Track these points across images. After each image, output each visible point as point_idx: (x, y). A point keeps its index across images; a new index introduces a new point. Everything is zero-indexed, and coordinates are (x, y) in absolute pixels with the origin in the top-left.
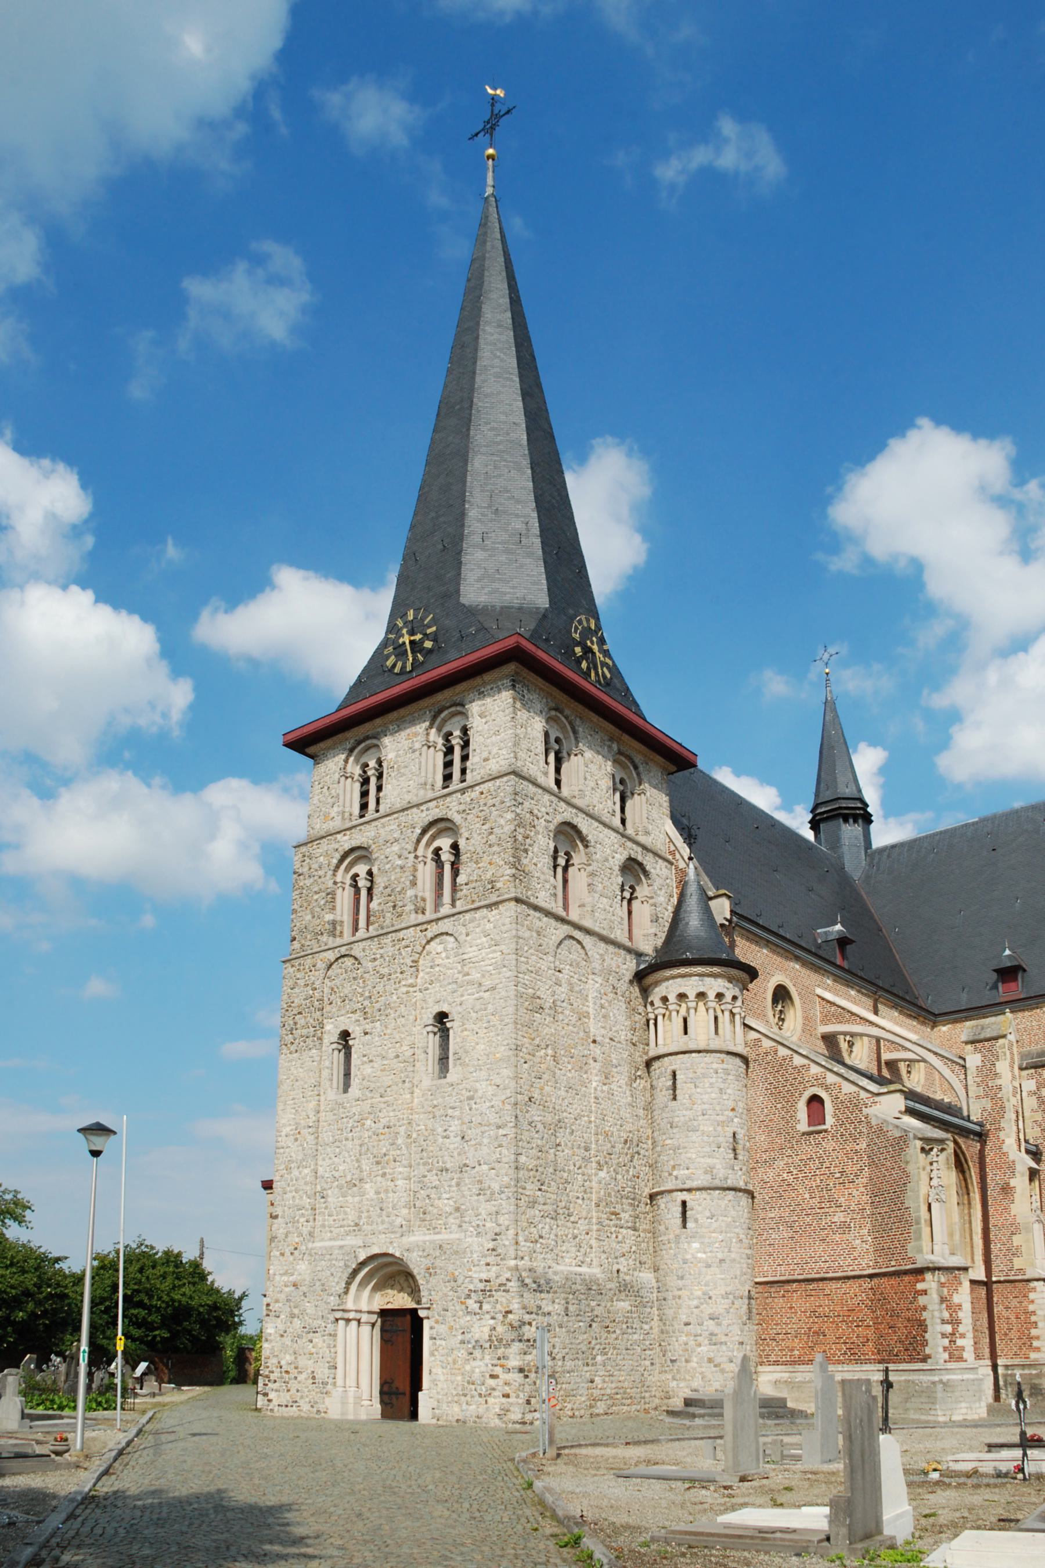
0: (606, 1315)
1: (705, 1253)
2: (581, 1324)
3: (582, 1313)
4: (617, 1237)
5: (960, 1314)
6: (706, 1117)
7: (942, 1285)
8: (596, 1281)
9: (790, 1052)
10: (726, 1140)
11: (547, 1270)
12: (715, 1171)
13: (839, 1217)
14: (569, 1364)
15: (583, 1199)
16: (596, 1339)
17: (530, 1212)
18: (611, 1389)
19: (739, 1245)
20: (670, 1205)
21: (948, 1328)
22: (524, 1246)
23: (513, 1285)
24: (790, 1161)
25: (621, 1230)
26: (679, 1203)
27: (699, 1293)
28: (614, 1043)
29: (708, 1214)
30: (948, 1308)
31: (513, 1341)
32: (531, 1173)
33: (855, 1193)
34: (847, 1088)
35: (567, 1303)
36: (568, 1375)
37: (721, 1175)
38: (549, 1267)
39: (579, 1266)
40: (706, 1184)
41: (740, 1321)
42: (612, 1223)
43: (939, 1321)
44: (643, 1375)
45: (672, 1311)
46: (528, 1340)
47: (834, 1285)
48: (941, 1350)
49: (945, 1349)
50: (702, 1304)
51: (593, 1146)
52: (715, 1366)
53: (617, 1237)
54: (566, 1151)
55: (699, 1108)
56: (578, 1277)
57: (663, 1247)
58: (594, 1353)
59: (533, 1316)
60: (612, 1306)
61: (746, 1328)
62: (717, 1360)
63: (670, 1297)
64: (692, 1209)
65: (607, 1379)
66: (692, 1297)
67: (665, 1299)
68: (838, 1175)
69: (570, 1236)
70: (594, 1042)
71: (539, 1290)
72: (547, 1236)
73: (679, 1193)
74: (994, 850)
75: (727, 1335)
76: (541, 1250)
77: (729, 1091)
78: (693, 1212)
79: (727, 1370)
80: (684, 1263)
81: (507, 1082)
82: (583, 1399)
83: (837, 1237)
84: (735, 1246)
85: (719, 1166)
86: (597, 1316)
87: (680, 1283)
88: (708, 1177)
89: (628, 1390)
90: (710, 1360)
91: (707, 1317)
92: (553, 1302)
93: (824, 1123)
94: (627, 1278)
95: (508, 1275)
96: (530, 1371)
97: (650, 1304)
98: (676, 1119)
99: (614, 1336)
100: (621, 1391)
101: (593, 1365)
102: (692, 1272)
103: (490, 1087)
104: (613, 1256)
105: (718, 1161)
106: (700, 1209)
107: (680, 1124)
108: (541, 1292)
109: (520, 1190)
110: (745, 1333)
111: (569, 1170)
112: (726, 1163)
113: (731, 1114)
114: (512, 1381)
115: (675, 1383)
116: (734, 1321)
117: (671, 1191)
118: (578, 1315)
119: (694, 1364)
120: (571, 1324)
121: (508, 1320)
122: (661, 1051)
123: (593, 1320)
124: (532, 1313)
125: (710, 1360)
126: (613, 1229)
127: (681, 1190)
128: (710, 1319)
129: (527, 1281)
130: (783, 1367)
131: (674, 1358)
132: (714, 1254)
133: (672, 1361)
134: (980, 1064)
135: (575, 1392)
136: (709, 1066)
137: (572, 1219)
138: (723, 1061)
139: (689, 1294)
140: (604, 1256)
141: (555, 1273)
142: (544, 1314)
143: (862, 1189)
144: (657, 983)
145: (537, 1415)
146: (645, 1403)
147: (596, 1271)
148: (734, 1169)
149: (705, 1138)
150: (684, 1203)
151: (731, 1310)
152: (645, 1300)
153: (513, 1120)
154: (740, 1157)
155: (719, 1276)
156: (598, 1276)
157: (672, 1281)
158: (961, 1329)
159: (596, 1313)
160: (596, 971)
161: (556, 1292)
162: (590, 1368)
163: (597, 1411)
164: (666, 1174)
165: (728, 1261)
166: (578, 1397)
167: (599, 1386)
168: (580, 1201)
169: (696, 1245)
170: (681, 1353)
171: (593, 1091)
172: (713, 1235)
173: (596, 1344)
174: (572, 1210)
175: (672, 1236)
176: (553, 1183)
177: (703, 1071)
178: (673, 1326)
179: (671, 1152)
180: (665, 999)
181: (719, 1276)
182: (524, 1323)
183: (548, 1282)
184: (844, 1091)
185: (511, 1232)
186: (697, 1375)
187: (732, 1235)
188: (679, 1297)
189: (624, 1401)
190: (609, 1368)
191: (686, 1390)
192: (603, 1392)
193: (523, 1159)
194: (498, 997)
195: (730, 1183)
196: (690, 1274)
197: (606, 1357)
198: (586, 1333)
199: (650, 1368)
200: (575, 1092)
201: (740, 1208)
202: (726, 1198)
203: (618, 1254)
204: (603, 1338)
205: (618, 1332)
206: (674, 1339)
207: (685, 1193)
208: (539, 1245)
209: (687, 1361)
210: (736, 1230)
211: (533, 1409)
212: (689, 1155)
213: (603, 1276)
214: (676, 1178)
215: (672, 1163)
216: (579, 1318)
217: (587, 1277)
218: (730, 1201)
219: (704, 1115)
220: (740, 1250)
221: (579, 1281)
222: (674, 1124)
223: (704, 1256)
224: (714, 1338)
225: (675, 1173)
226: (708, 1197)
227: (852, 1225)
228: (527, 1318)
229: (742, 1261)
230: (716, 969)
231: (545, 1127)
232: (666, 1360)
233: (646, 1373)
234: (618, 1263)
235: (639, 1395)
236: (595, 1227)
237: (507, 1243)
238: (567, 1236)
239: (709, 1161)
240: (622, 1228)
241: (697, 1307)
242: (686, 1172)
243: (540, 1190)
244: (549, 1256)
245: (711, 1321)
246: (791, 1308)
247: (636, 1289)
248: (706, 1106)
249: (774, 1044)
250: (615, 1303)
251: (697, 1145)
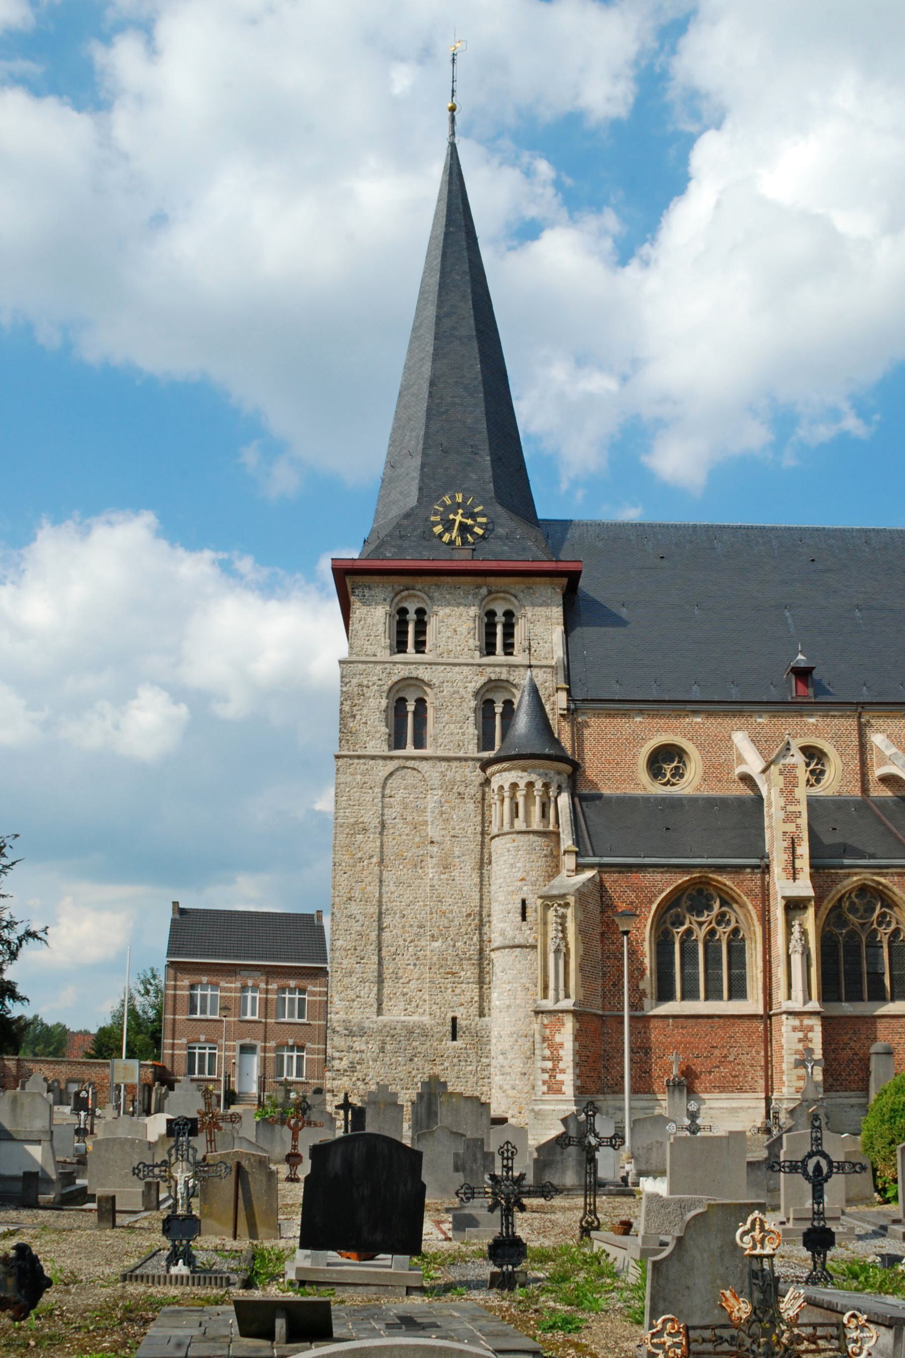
4: (453, 991)
5: (561, 1052)
7: (545, 1026)
16: (418, 1070)
21: (549, 1065)
30: (549, 1047)
43: (540, 1058)
46: (338, 1070)
48: (540, 1083)
49: (544, 1082)
71: (351, 1034)
77: (518, 865)
84: (520, 994)
85: (508, 929)
99: (442, 1067)
108: (354, 1036)
113: (519, 883)
120: (387, 1059)
129: (338, 1029)
140: (434, 1007)
147: (426, 1019)
158: (562, 1065)
159: (419, 1050)
162: (410, 1091)
168: (411, 967)
195: (517, 942)
198: (405, 1065)
210: (522, 981)
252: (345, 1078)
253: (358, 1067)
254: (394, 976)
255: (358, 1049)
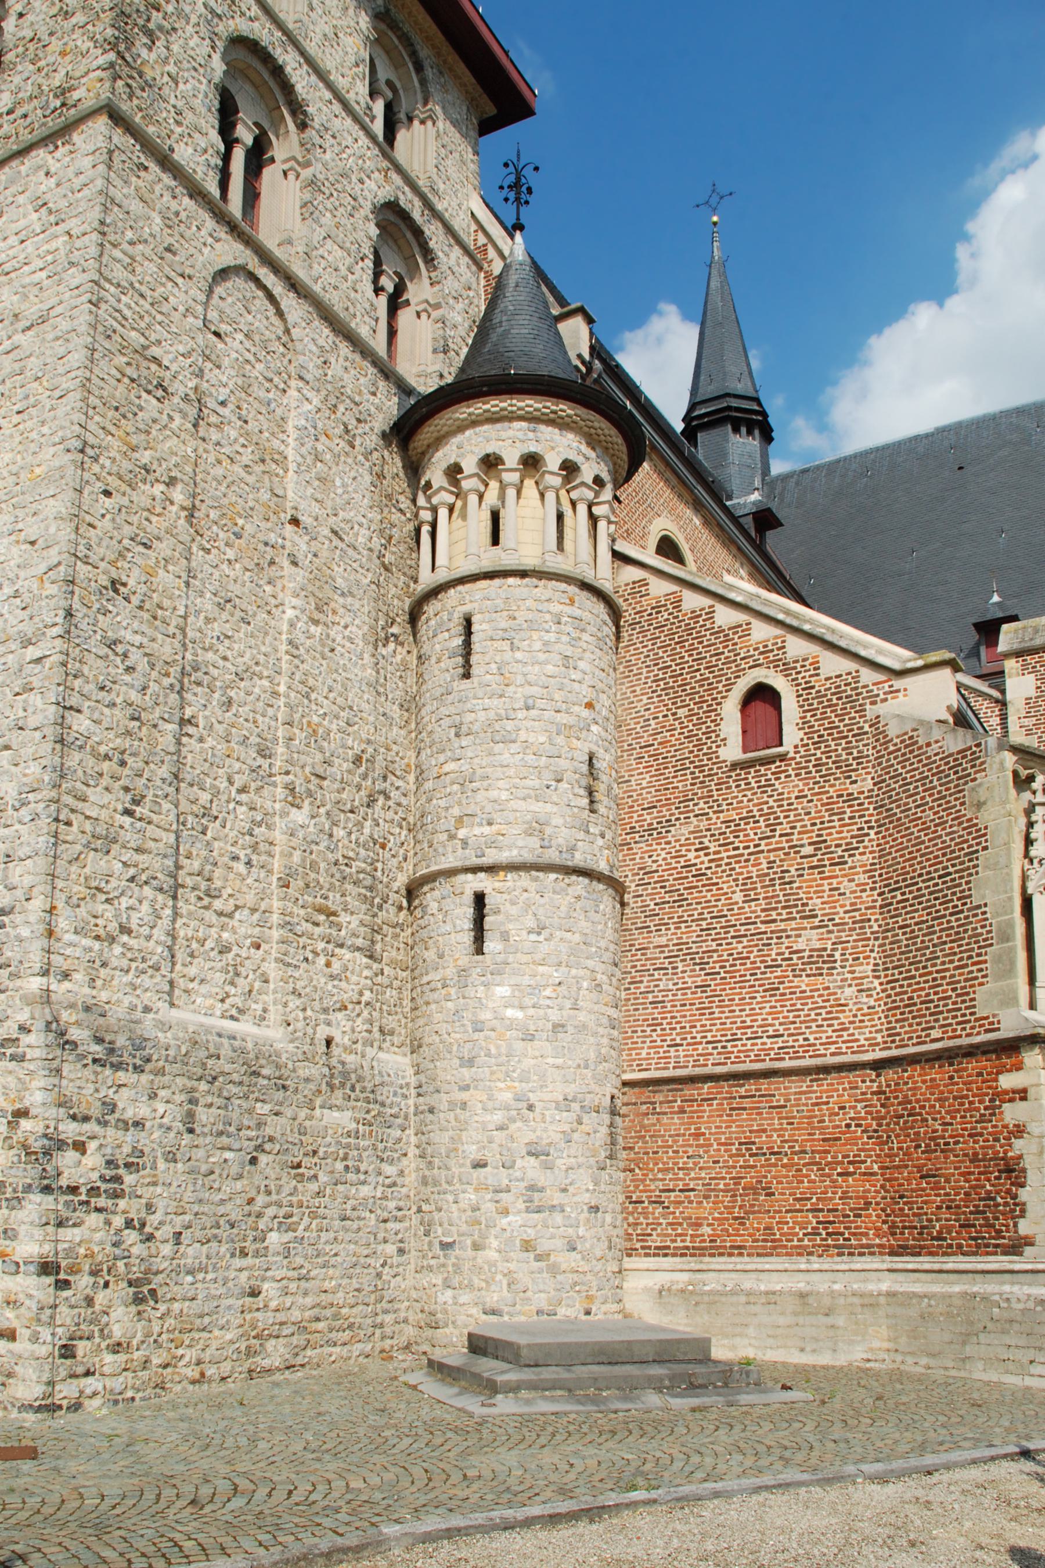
0: (295, 1138)
1: (522, 1008)
2: (228, 1155)
3: (232, 1129)
4: (328, 965)
6: (533, 713)
8: (273, 1058)
9: (706, 602)
10: (573, 766)
11: (138, 1014)
12: (548, 831)
13: (809, 940)
14: (192, 1253)
15: (249, 863)
16: (269, 1193)
17: (95, 863)
18: (303, 1309)
19: (594, 995)
20: (447, 904)
22: (71, 944)
23: (34, 1042)
24: (704, 824)
25: (337, 951)
26: (469, 898)
27: (508, 1096)
28: (340, 545)
29: (531, 923)
31: (28, 1189)
32: (106, 766)
33: (846, 886)
34: (833, 665)
35: (193, 1101)
36: (189, 1279)
37: (560, 841)
38: (147, 1009)
39: (232, 1018)
40: (528, 857)
41: (592, 1161)
42: (317, 930)
44: (379, 1275)
45: (445, 1136)
46: (73, 1190)
47: (794, 1086)
50: (513, 1120)
51: (281, 749)
52: (539, 1258)
53: (328, 965)
54: (210, 742)
55: (518, 693)
56: (225, 1041)
57: (435, 996)
58: (262, 1226)
59: (91, 1127)
60: (310, 1118)
61: (605, 1176)
62: (544, 1246)
63: (444, 1106)
64: (497, 912)
65: (293, 1286)
66: (490, 1105)
67: (431, 1111)
68: (808, 850)
69: (209, 944)
70: (295, 521)
72: (145, 931)
73: (470, 876)
74: (960, 468)
75: (564, 1190)
76: (125, 963)
78: (500, 918)
79: (564, 1267)
80: (475, 1030)
81: (52, 530)
82: (229, 1336)
83: (803, 983)
85: (557, 821)
86: (271, 1139)
87: (466, 1073)
88: (534, 842)
89: (344, 1311)
90: (527, 1246)
91: (524, 1152)
92: (152, 1096)
93: (781, 745)
94: (350, 1059)
95: (23, 1016)
96: (74, 1270)
97: (399, 1121)
98: (469, 717)
99: (314, 1187)
100: (328, 1313)
101: (257, 1254)
102: (493, 1051)
103: (15, 550)
104: (317, 1005)
105: (555, 809)
106: (514, 910)
107: (475, 727)
108: (117, 1067)
109: (68, 800)
110: (603, 1187)
111: (213, 786)
112: (574, 816)
113: (585, 713)
114: (21, 1297)
115: (449, 1293)
116: (581, 1160)
117: (451, 873)
118: (221, 1133)
119: (491, 1254)
120: (200, 1153)
121: (19, 1136)
122: (443, 575)
123: (260, 1148)
124: (86, 1119)
125: (527, 1246)
126: (321, 945)
127: (475, 870)
128: (530, 1154)
130: (678, 1259)
131: (450, 1240)
132: (541, 1012)
133: (445, 1246)
134: (1032, 693)
135: (207, 1320)
136: (545, 606)
137: (218, 904)
138: (572, 601)
139: (484, 1098)
140: (294, 1002)
141: (165, 1026)
142: (125, 1125)
143: (862, 878)
144: (439, 441)
145: (92, 1384)
146: (383, 1338)
147: (274, 1034)
148: (588, 832)
149: (530, 758)
150: (479, 899)
151: (576, 1136)
152: (389, 1111)
153: (60, 620)
154: (602, 810)
155: (550, 1060)
156: (278, 1046)
157: (448, 1070)
159: (269, 1131)
160: (308, 377)
161: (161, 1072)
162: (249, 1261)
163: (266, 1363)
164: (444, 837)
165: (570, 1029)
166: (217, 1332)
167: (273, 1304)
168: (240, 867)
169: (502, 991)
170: (464, 1228)
171: (285, 628)
172: (541, 968)
173: (267, 1206)
174: (218, 883)
175: (450, 972)
176: (166, 806)
177: (530, 616)
178: (448, 1169)
179: (456, 787)
180: (454, 472)
181: (550, 1060)
182: (61, 1145)
183: (139, 1044)
184: (824, 672)
185: (38, 903)
186: (499, 1277)
187: (581, 972)
188: (464, 1105)
189: (333, 1335)
190: (299, 1261)
191: (474, 1311)
192: (281, 1317)
193: (80, 723)
194: (50, 336)
195: (578, 859)
196: (488, 1055)
197: (291, 1234)
198: (240, 1177)
199: (395, 1260)
200: (238, 614)
201: (598, 917)
202: (570, 890)
203: (328, 1002)
204: (286, 1190)
205: (323, 1178)
206: (450, 1198)
207: (482, 875)
208: (117, 950)
209: (476, 1247)
210: (590, 963)
211: (80, 1370)
212: (493, 794)
213: (291, 1047)
214: (465, 843)
215: (456, 811)
216: (224, 1140)
217: (250, 1046)
218: (578, 898)
219: (528, 709)
220: (596, 1007)
221: (226, 1051)
222: (464, 729)
223: (520, 1014)
224: (536, 1196)
225: (462, 833)
226: (532, 886)
227: (837, 955)
228: (70, 1130)
229: (601, 1030)
230: (565, 409)
231: (152, 666)
232: (430, 1243)
233: (387, 1269)
234: (329, 1024)
235: (369, 1321)
236: (276, 934)
237: (25, 932)
238: (202, 942)
239: (538, 807)
240: (341, 946)
241: (501, 1128)
242: (486, 830)
243: (128, 812)
244: (146, 981)
245: (532, 1159)
246: (697, 1135)
247: (369, 1086)
248: (535, 690)
249: (675, 588)
250: (318, 1112)
251: (511, 772)
252: (94, 1220)
253: (129, 1179)
254: (204, 885)
255: (129, 1114)
